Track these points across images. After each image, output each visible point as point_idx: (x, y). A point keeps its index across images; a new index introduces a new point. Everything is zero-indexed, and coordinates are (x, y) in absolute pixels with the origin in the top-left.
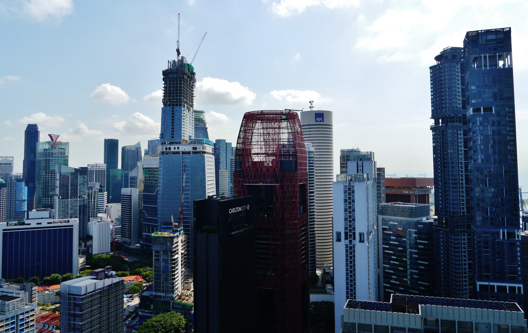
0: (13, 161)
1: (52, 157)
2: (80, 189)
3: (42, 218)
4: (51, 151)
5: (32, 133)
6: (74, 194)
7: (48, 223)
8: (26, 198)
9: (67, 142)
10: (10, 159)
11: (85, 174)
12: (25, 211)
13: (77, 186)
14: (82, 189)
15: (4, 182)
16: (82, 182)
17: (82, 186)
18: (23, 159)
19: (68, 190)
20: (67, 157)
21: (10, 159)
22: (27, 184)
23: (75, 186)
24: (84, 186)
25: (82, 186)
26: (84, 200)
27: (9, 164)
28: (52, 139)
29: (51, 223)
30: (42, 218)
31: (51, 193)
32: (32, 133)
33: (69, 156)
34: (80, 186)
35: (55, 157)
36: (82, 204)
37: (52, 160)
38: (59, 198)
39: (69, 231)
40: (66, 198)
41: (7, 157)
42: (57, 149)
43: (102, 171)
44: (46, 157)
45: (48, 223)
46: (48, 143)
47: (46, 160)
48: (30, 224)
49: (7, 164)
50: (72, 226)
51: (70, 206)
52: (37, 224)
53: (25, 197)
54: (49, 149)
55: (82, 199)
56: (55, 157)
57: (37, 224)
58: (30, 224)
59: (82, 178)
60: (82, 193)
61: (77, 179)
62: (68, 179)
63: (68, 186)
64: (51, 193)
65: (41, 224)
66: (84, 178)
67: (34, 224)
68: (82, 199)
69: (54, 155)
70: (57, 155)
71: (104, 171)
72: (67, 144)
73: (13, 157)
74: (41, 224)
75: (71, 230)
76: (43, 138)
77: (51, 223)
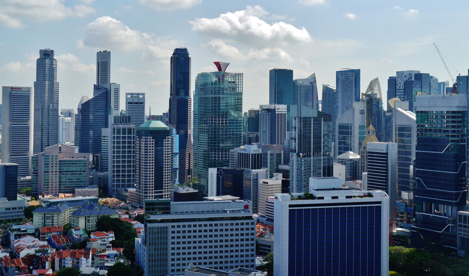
0: (144, 98)
1: (223, 94)
2: (324, 142)
3: (334, 189)
4: (221, 86)
5: (181, 60)
6: (317, 149)
7: (347, 197)
8: (178, 151)
9: (240, 72)
10: (141, 96)
11: (330, 120)
12: (176, 169)
13: (320, 138)
14: (326, 143)
15: (168, 129)
16: (326, 132)
17: (326, 137)
18: (168, 96)
19: (310, 144)
20: (241, 94)
21: (141, 96)
22: (178, 133)
23: (318, 137)
24: (328, 137)
25: (326, 137)
26: (328, 159)
27: (140, 103)
28: (220, 69)
29: (350, 197)
30: (334, 189)
31: (221, 145)
32: (181, 60)
33: (243, 93)
34: (324, 137)
35: (227, 94)
36: (327, 165)
37: (223, 98)
38: (298, 155)
39: (375, 210)
40: (308, 156)
41: (138, 94)
42: (226, 83)
43: (281, 114)
44: (215, 93)
45: (347, 197)
46: (215, 74)
47: (215, 98)
48: (322, 198)
49: (137, 103)
50: (380, 203)
51: (312, 168)
52: (333, 198)
53: (176, 149)
54: (215, 83)
55: (327, 157)
56: (227, 94)
57: (333, 198)
58: (322, 198)
59: (326, 126)
60: (326, 148)
61: (321, 127)
62: (311, 127)
63: (311, 138)
64: (221, 145)
65: (337, 198)
66: (329, 126)
67: (328, 199)
68: (327, 157)
69: (225, 92)
70: (229, 92)
71: (285, 114)
72: (240, 75)
73: (143, 94)
74: (337, 198)
75: (379, 209)
76: (199, 67)
77: (350, 197)
